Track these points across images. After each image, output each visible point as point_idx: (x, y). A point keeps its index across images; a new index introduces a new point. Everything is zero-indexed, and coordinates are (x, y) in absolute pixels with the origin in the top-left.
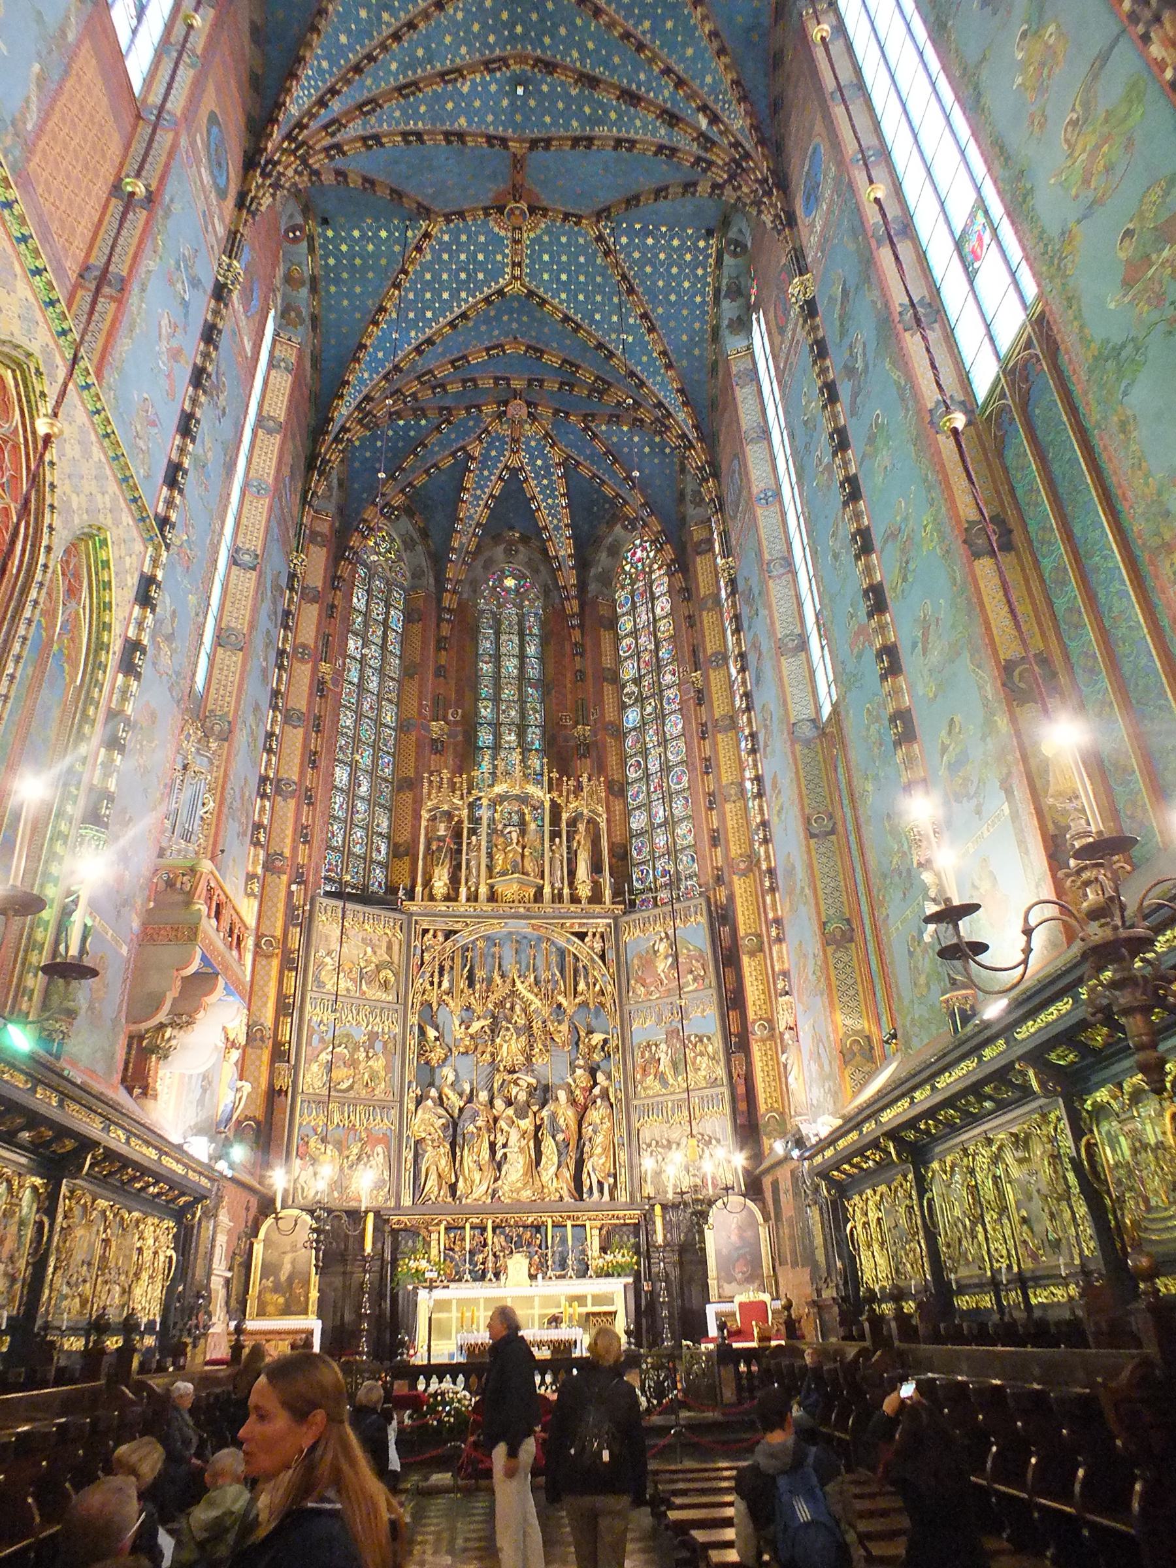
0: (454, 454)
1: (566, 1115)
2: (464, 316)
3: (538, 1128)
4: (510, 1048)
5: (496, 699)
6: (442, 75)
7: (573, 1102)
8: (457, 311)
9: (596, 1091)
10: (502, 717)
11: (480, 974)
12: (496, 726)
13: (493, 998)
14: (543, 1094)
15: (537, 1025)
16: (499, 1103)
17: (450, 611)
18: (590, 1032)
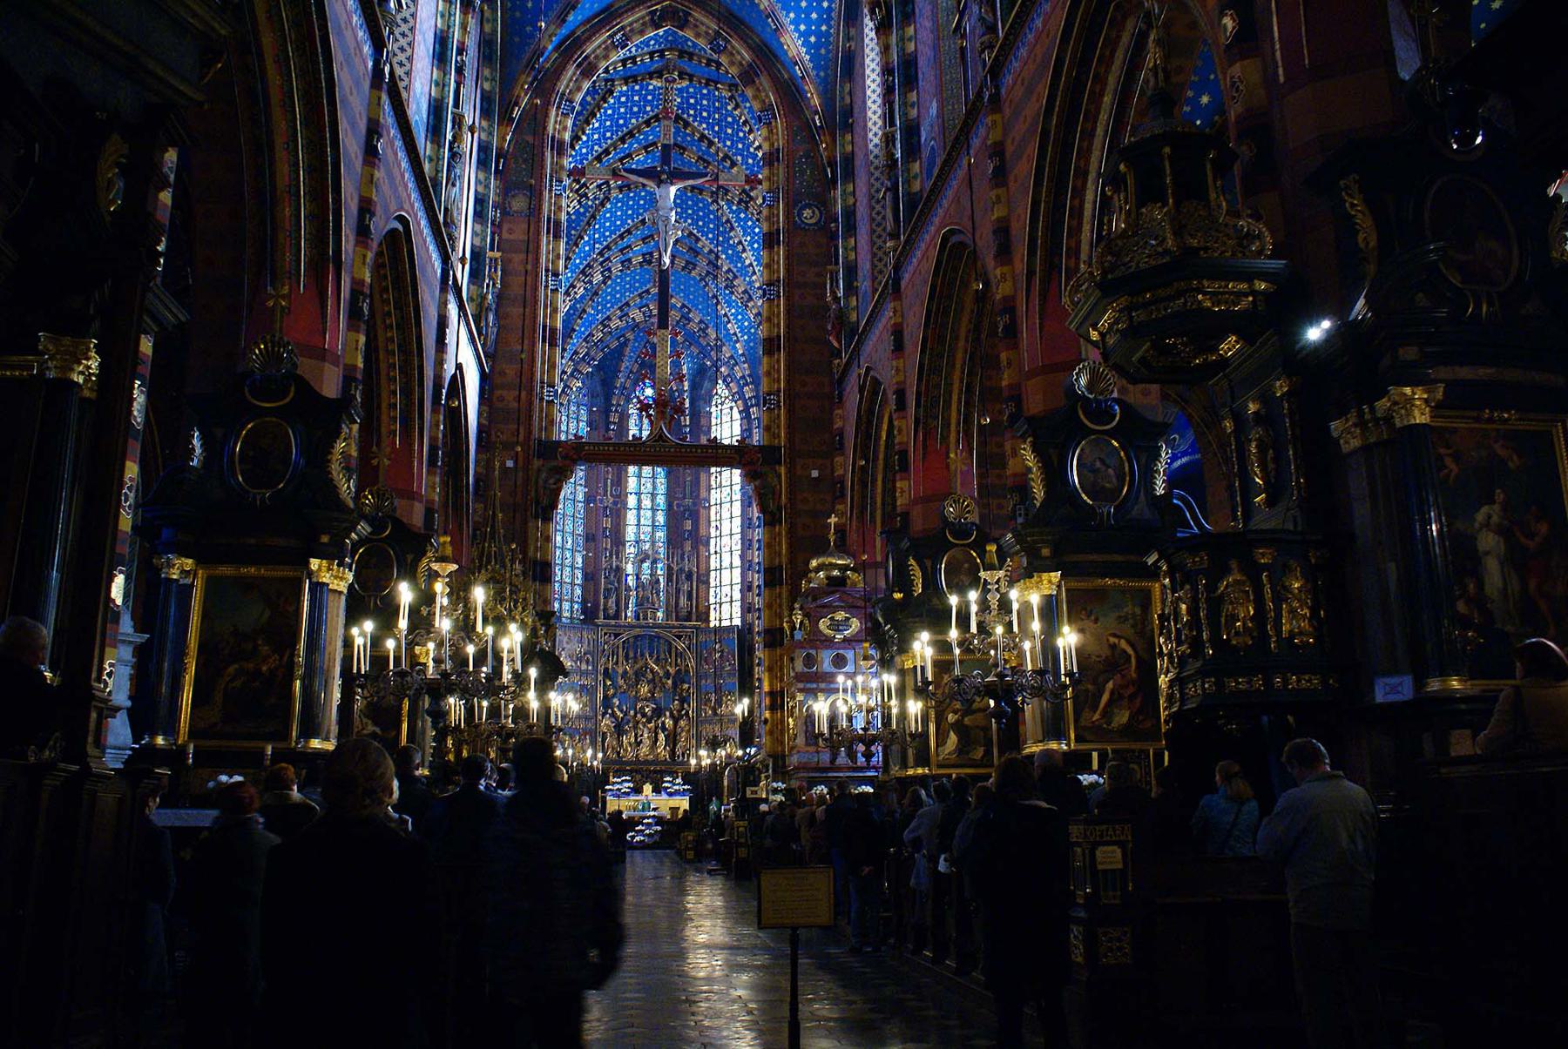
0: (618, 339)
1: (669, 723)
2: (627, 304)
3: (656, 727)
4: (644, 689)
5: (639, 476)
6: (621, 250)
7: (672, 716)
8: (624, 302)
9: (683, 712)
10: (642, 488)
11: (631, 655)
12: (639, 494)
13: (638, 666)
14: (658, 712)
15: (657, 679)
16: (639, 715)
17: (614, 423)
18: (683, 682)
